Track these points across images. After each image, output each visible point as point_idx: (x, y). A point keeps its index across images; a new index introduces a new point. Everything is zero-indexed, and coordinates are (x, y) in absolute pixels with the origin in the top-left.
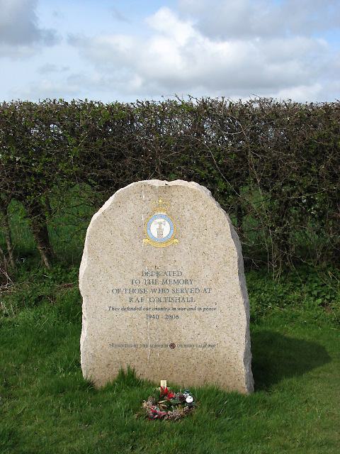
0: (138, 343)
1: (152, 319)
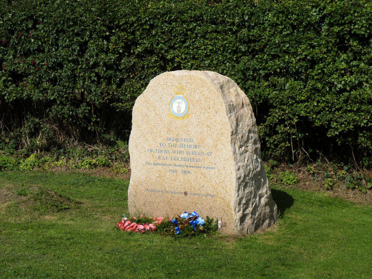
0: (164, 189)
1: (173, 172)
